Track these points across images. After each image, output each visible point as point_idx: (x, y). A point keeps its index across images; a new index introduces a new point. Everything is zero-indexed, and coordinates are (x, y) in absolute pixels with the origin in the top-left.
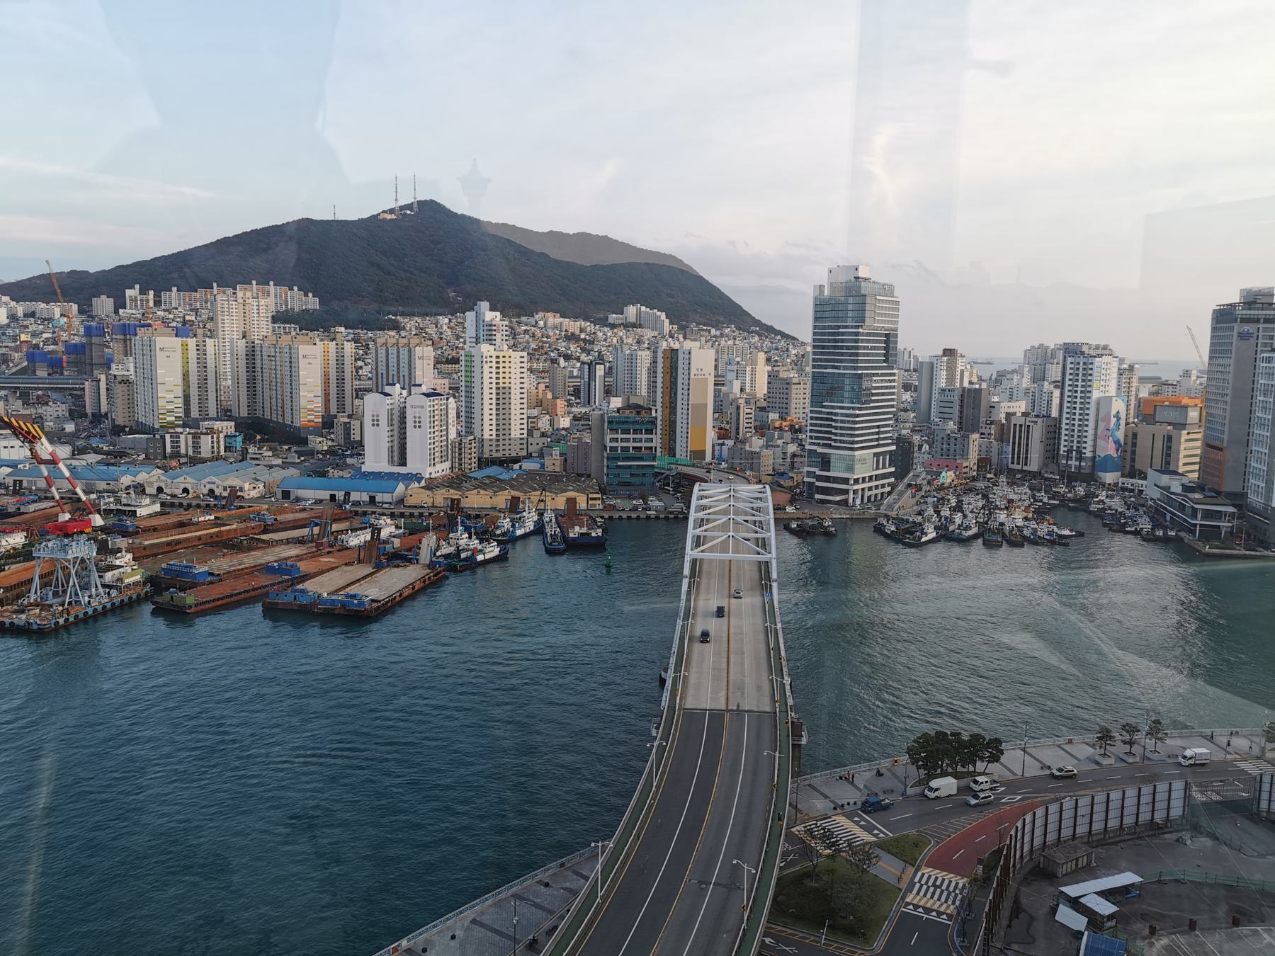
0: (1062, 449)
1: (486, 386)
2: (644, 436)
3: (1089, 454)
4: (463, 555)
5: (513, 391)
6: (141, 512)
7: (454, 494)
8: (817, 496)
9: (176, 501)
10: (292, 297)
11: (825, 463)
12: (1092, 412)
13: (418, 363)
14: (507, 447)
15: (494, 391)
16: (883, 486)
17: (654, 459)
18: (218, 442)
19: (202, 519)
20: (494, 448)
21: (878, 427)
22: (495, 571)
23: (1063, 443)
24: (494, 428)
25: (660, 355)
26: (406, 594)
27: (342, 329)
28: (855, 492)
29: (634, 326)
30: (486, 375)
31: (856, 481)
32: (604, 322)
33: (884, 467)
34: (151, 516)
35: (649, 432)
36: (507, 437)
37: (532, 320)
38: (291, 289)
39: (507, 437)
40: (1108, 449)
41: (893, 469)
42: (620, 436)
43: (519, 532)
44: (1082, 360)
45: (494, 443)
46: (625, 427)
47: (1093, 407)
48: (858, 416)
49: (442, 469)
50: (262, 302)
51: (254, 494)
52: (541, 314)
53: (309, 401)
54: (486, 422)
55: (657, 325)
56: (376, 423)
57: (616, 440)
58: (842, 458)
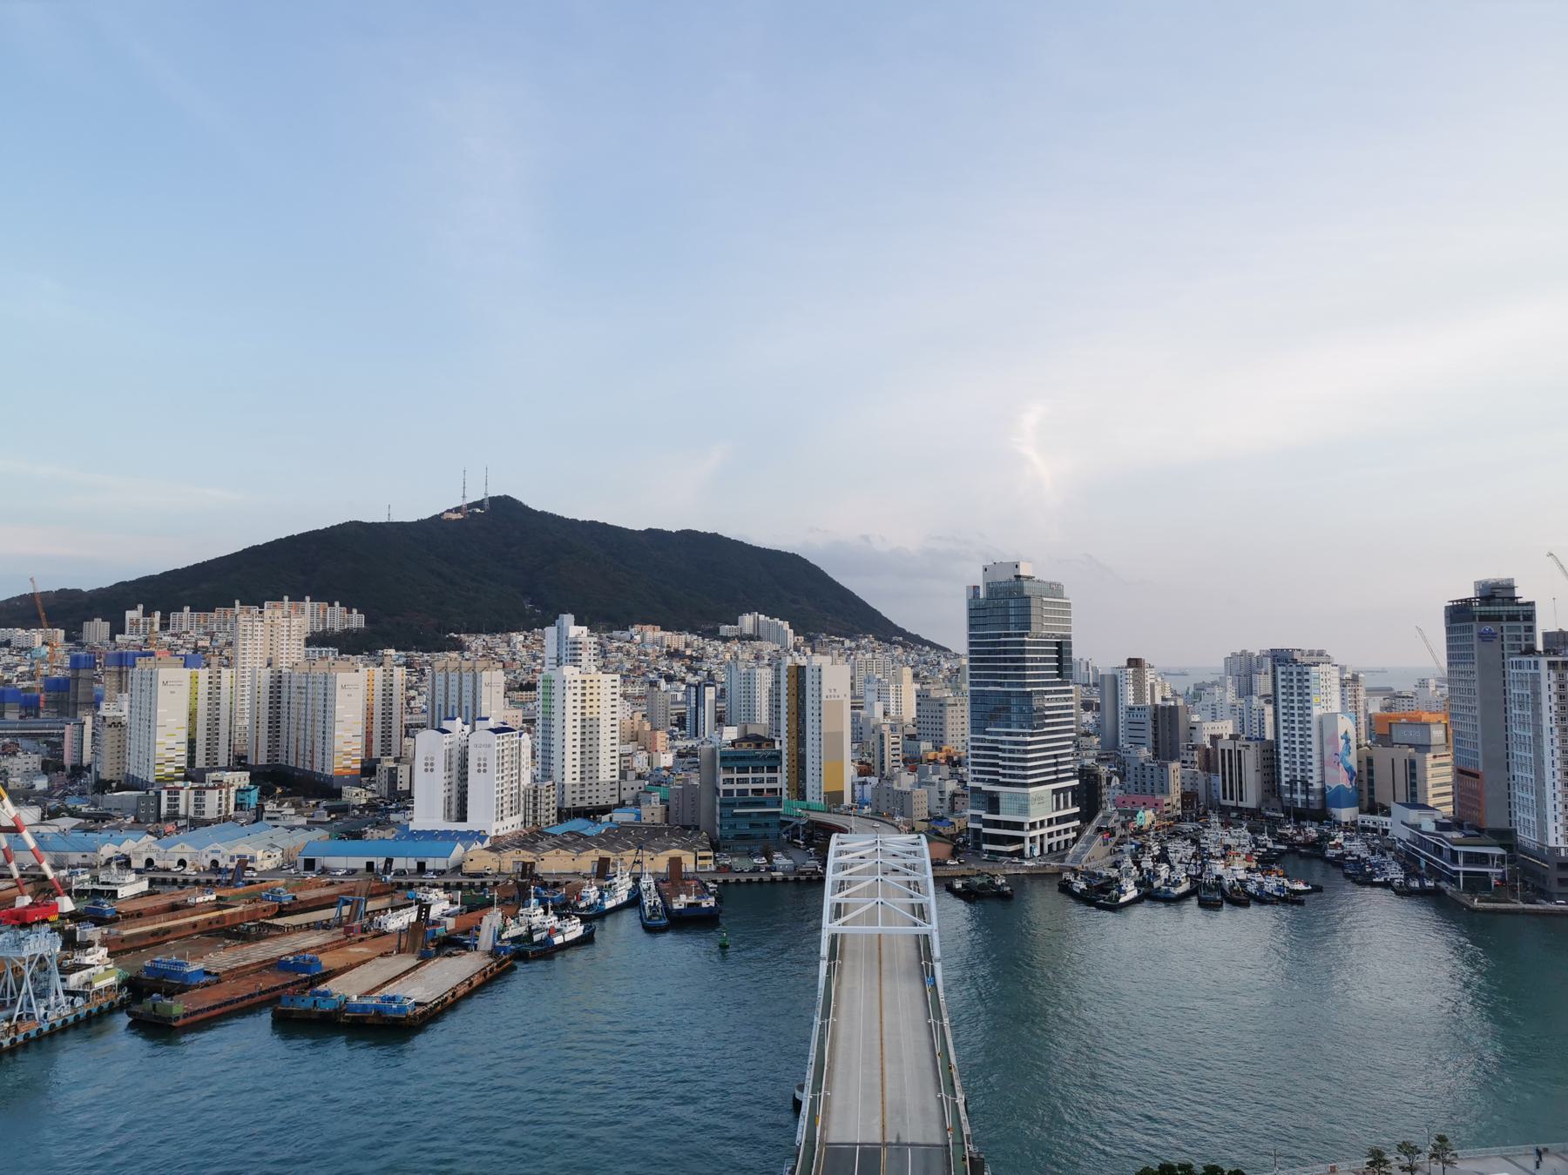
0: (1284, 779)
1: (569, 717)
2: (766, 775)
3: (1317, 786)
4: (536, 938)
5: (601, 722)
6: (123, 892)
7: (526, 856)
8: (985, 847)
9: (169, 877)
10: (332, 614)
11: (993, 803)
12: (1315, 732)
13: (485, 692)
14: (594, 794)
15: (578, 724)
16: (1066, 831)
17: (779, 803)
18: (227, 799)
19: (199, 900)
20: (578, 796)
21: (1055, 756)
22: (580, 955)
23: (1284, 772)
24: (578, 769)
25: (784, 673)
26: (460, 993)
27: (392, 652)
28: (1032, 840)
29: (751, 638)
30: (569, 704)
31: (1033, 826)
32: (714, 634)
33: (1066, 807)
34: (136, 897)
35: (773, 769)
36: (594, 781)
37: (626, 635)
38: (331, 605)
39: (594, 781)
40: (1340, 779)
41: (1077, 810)
42: (736, 776)
43: (609, 904)
44: (1295, 670)
45: (578, 789)
46: (740, 764)
47: (1314, 726)
48: (1030, 743)
49: (511, 824)
50: (295, 621)
51: (268, 865)
52: (637, 628)
53: (345, 745)
54: (569, 763)
55: (779, 637)
56: (430, 768)
57: (731, 781)
58: (1014, 797)
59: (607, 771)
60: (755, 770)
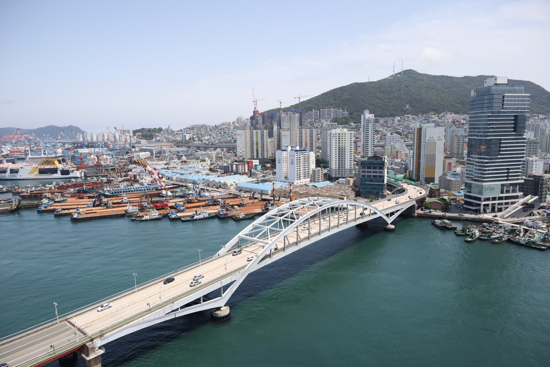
2: (378, 170)
20: (337, 173)
21: (507, 169)
42: (367, 170)
45: (337, 171)
52: (444, 113)
57: (365, 172)
58: (477, 186)
59: (348, 164)
60: (374, 168)
